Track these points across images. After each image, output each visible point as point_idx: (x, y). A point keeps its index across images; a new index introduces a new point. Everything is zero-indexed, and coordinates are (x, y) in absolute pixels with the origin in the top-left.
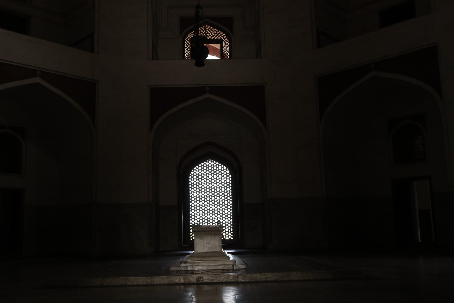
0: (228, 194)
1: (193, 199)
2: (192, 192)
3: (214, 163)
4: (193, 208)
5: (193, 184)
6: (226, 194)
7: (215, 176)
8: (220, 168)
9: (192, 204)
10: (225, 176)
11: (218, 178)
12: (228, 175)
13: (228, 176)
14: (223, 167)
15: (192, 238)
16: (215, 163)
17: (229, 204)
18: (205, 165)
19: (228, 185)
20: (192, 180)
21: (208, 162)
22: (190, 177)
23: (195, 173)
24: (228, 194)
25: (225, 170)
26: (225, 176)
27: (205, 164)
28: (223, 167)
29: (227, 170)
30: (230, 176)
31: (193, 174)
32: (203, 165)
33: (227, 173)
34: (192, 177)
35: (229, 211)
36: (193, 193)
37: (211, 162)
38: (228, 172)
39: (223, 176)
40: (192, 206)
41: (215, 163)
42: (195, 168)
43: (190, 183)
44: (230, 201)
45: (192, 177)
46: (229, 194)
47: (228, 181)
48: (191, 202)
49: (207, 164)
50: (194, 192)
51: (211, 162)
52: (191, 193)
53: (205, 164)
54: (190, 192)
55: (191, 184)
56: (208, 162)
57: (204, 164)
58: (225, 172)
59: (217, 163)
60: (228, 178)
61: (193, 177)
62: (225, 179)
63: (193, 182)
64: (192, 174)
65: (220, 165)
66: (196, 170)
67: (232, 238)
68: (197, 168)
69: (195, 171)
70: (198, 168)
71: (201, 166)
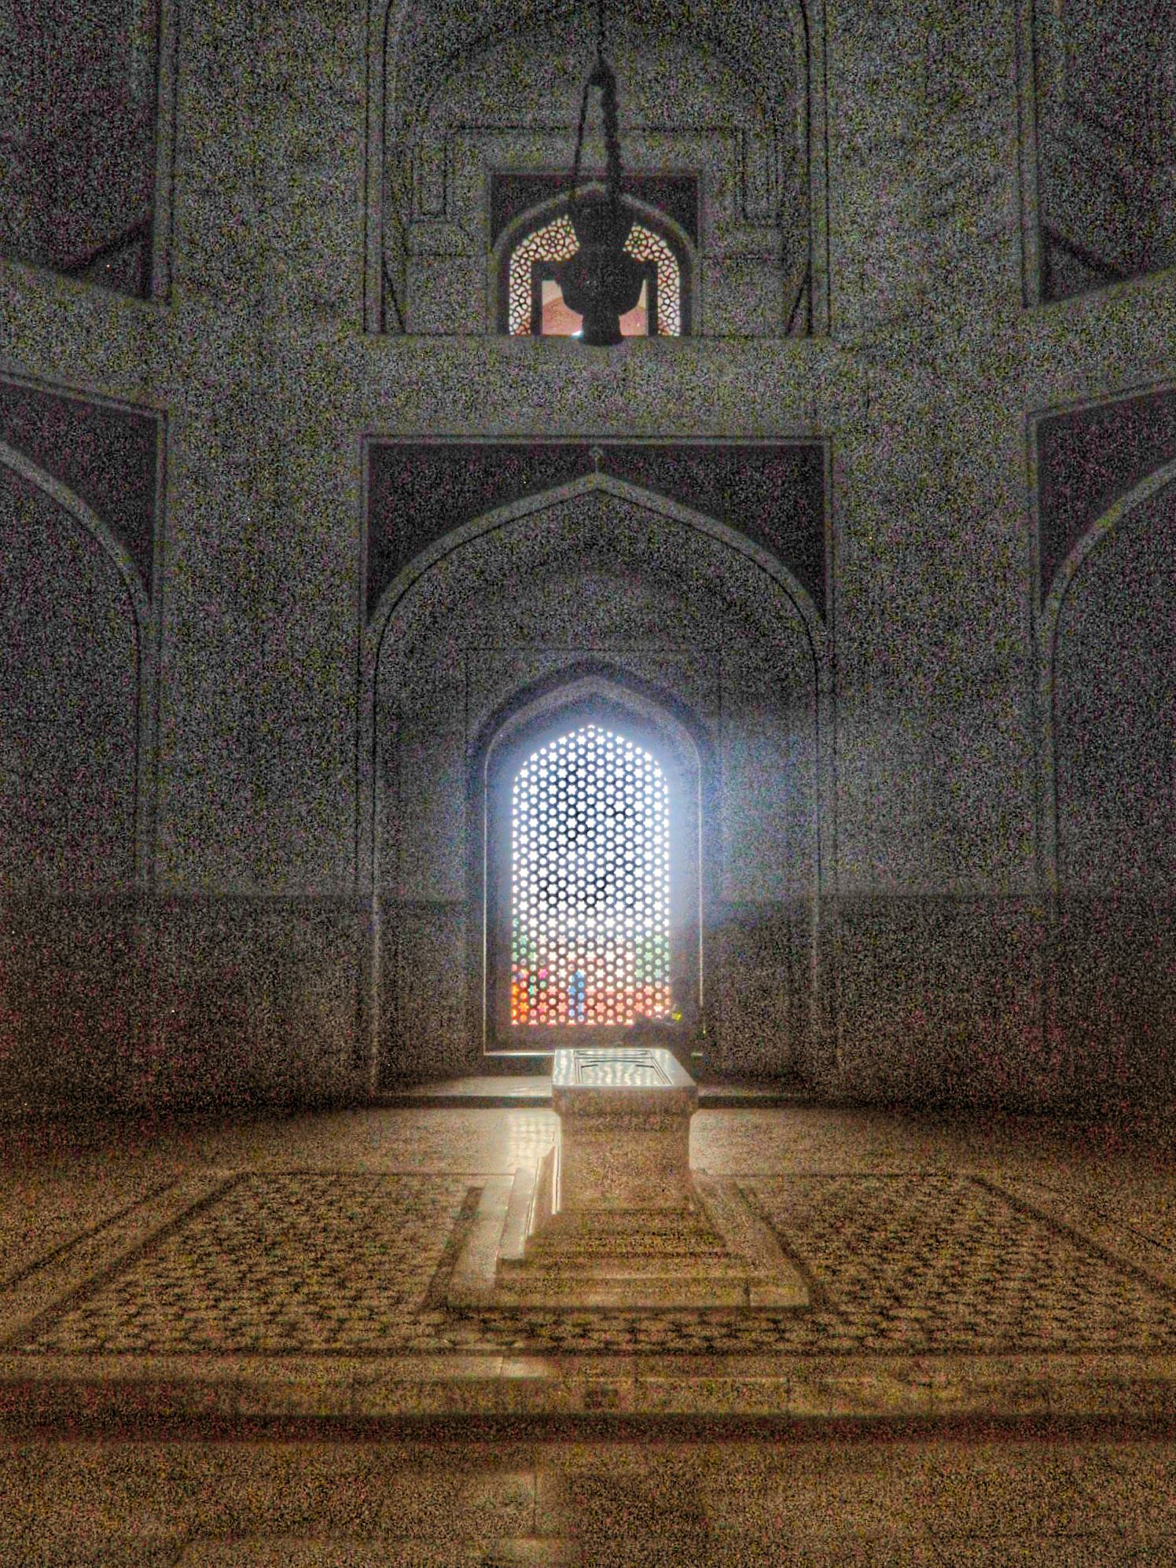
3: (608, 740)
13: (660, 790)
14: (641, 756)
15: (517, 1018)
16: (612, 740)
19: (659, 823)
20: (521, 800)
21: (585, 734)
29: (654, 767)
34: (522, 790)
36: (524, 850)
37: (597, 734)
40: (520, 899)
41: (612, 740)
42: (534, 757)
44: (664, 883)
45: (522, 790)
48: (518, 883)
49: (582, 740)
51: (597, 734)
54: (515, 845)
55: (518, 816)
56: (585, 734)
57: (570, 740)
64: (521, 780)
65: (629, 745)
68: (541, 757)
69: (534, 768)
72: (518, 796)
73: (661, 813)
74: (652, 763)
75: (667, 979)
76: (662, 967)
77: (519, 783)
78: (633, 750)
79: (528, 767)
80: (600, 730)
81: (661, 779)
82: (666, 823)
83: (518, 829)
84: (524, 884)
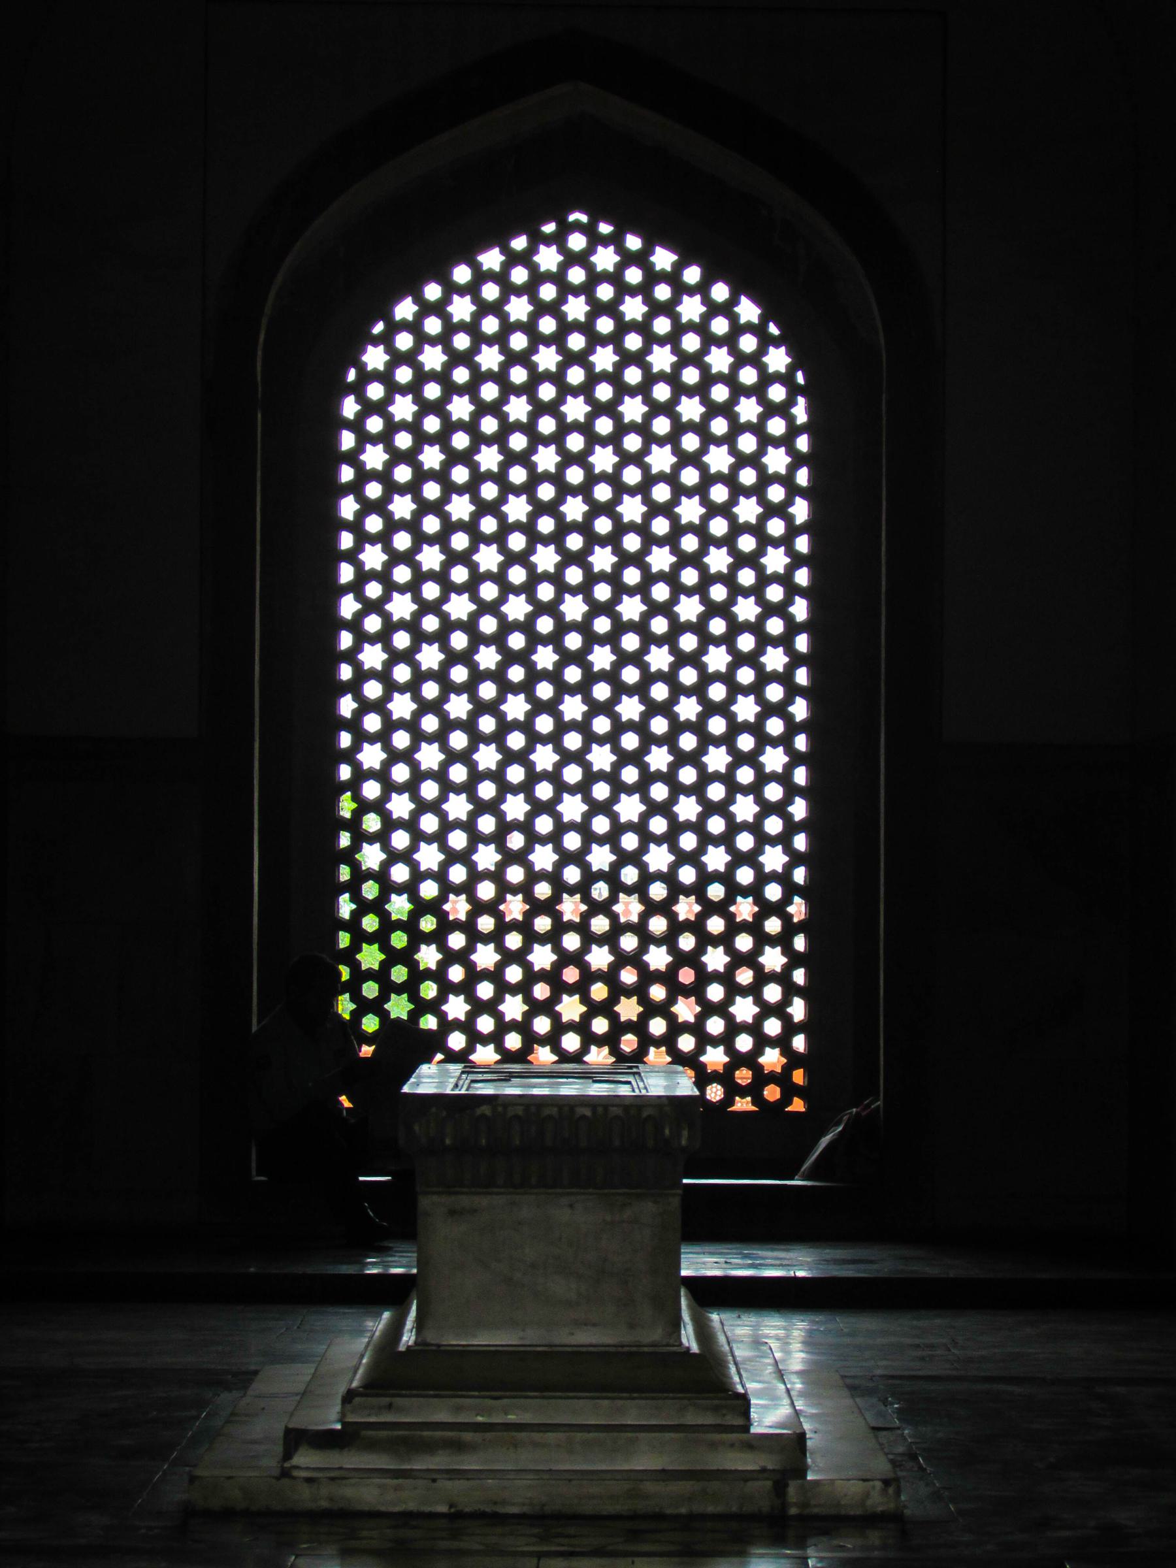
0: (769, 610)
1: (373, 657)
2: (363, 577)
3: (628, 259)
4: (372, 756)
5: (374, 490)
6: (747, 609)
7: (633, 409)
8: (691, 308)
9: (365, 706)
10: (748, 409)
11: (661, 425)
12: (777, 393)
13: (783, 409)
16: (641, 259)
17: (775, 726)
18: (519, 275)
20: (365, 438)
21: (558, 241)
22: (350, 408)
23: (410, 358)
24: (769, 610)
25: (748, 343)
26: (748, 409)
27: (525, 258)
28: (727, 309)
29: (766, 341)
30: (800, 412)
31: (386, 377)
32: (501, 278)
33: (766, 379)
34: (369, 408)
35: (779, 809)
38: (778, 360)
39: (727, 410)
40: (361, 737)
41: (641, 259)
42: (405, 310)
43: (347, 474)
44: (793, 691)
45: (369, 408)
46: (780, 610)
47: (777, 460)
49: (548, 258)
50: (384, 576)
51: (595, 240)
52: (357, 588)
53: (525, 258)
55: (356, 488)
57: (513, 259)
58: (741, 359)
59: (663, 259)
60: (776, 426)
61: (381, 408)
62: (747, 443)
63: (375, 457)
64: (366, 377)
65: (692, 275)
66: (415, 327)
67: (798, 1105)
68: (427, 309)
69: (404, 341)
70: (439, 309)
71: (472, 289)
72: (357, 425)
73: (787, 481)
74: (758, 330)
75: (799, 976)
76: (783, 1042)
77: (358, 389)
78: (702, 289)
79: (386, 340)
80: (605, 229)
81: (786, 379)
82: (801, 510)
83: (356, 527)
84: (372, 690)
